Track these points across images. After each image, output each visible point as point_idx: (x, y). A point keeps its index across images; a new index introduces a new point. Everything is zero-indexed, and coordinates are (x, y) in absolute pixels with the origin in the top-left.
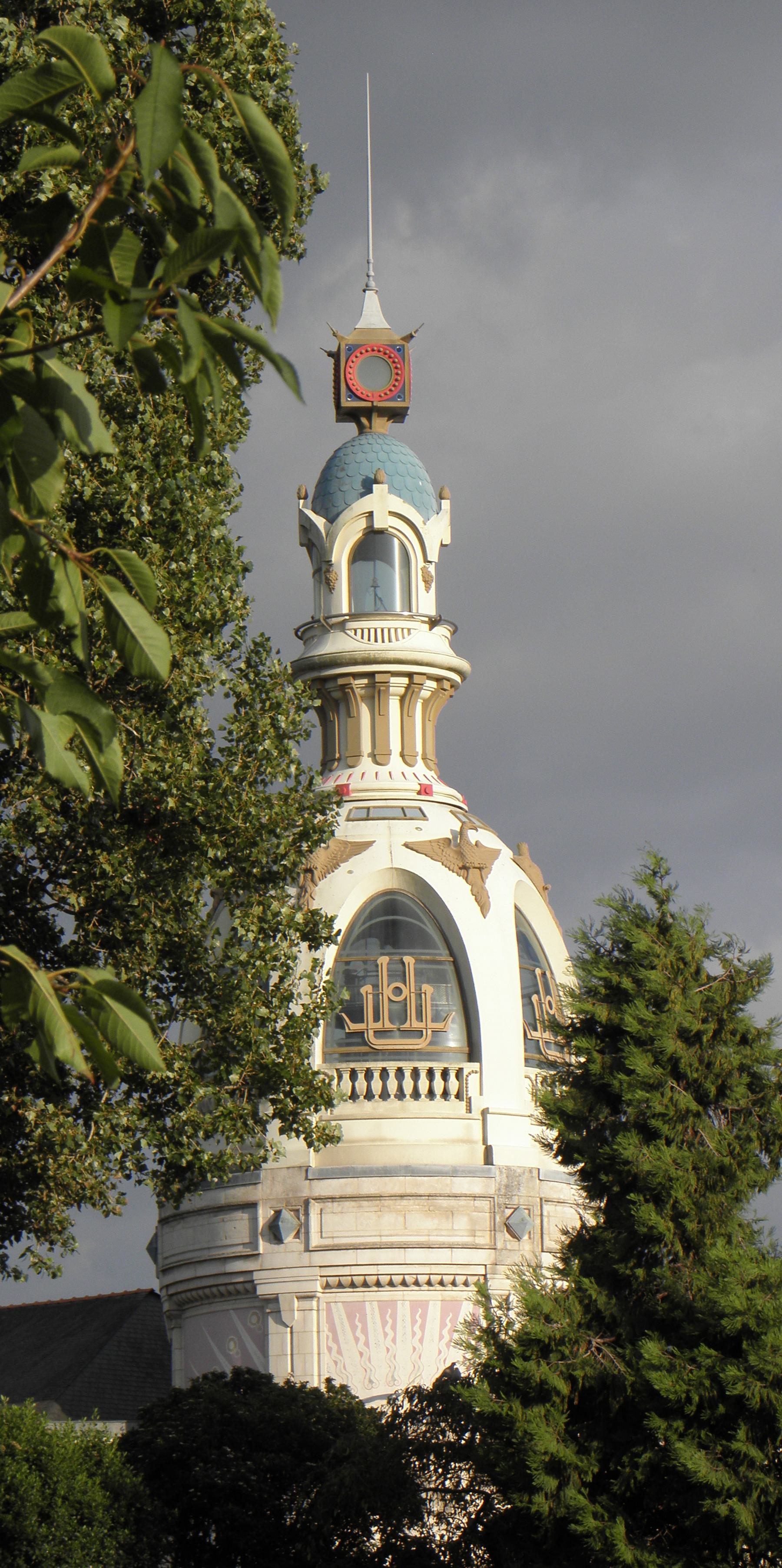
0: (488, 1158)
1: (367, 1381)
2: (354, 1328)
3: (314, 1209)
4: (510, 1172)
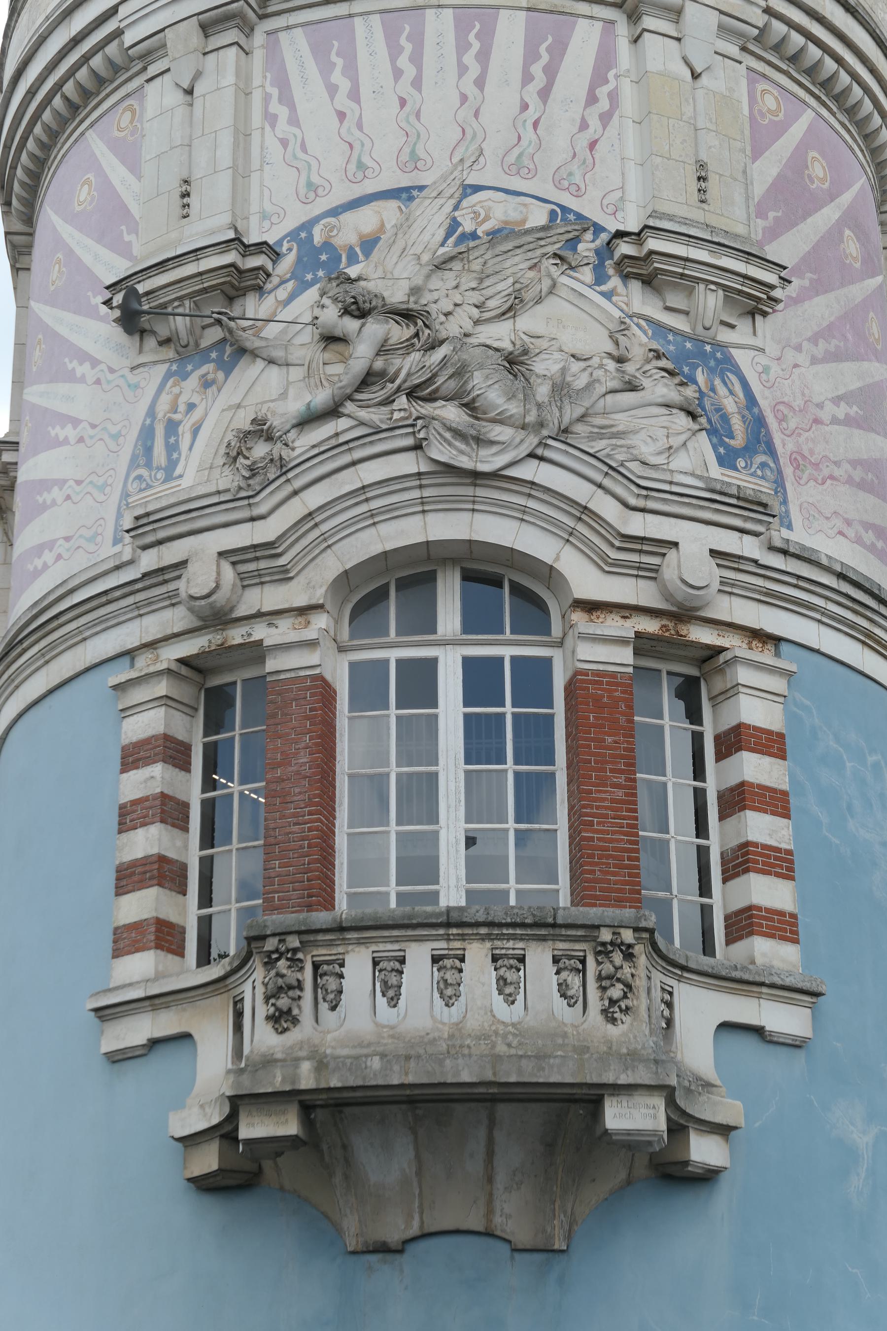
1: (352, 167)
2: (326, 68)
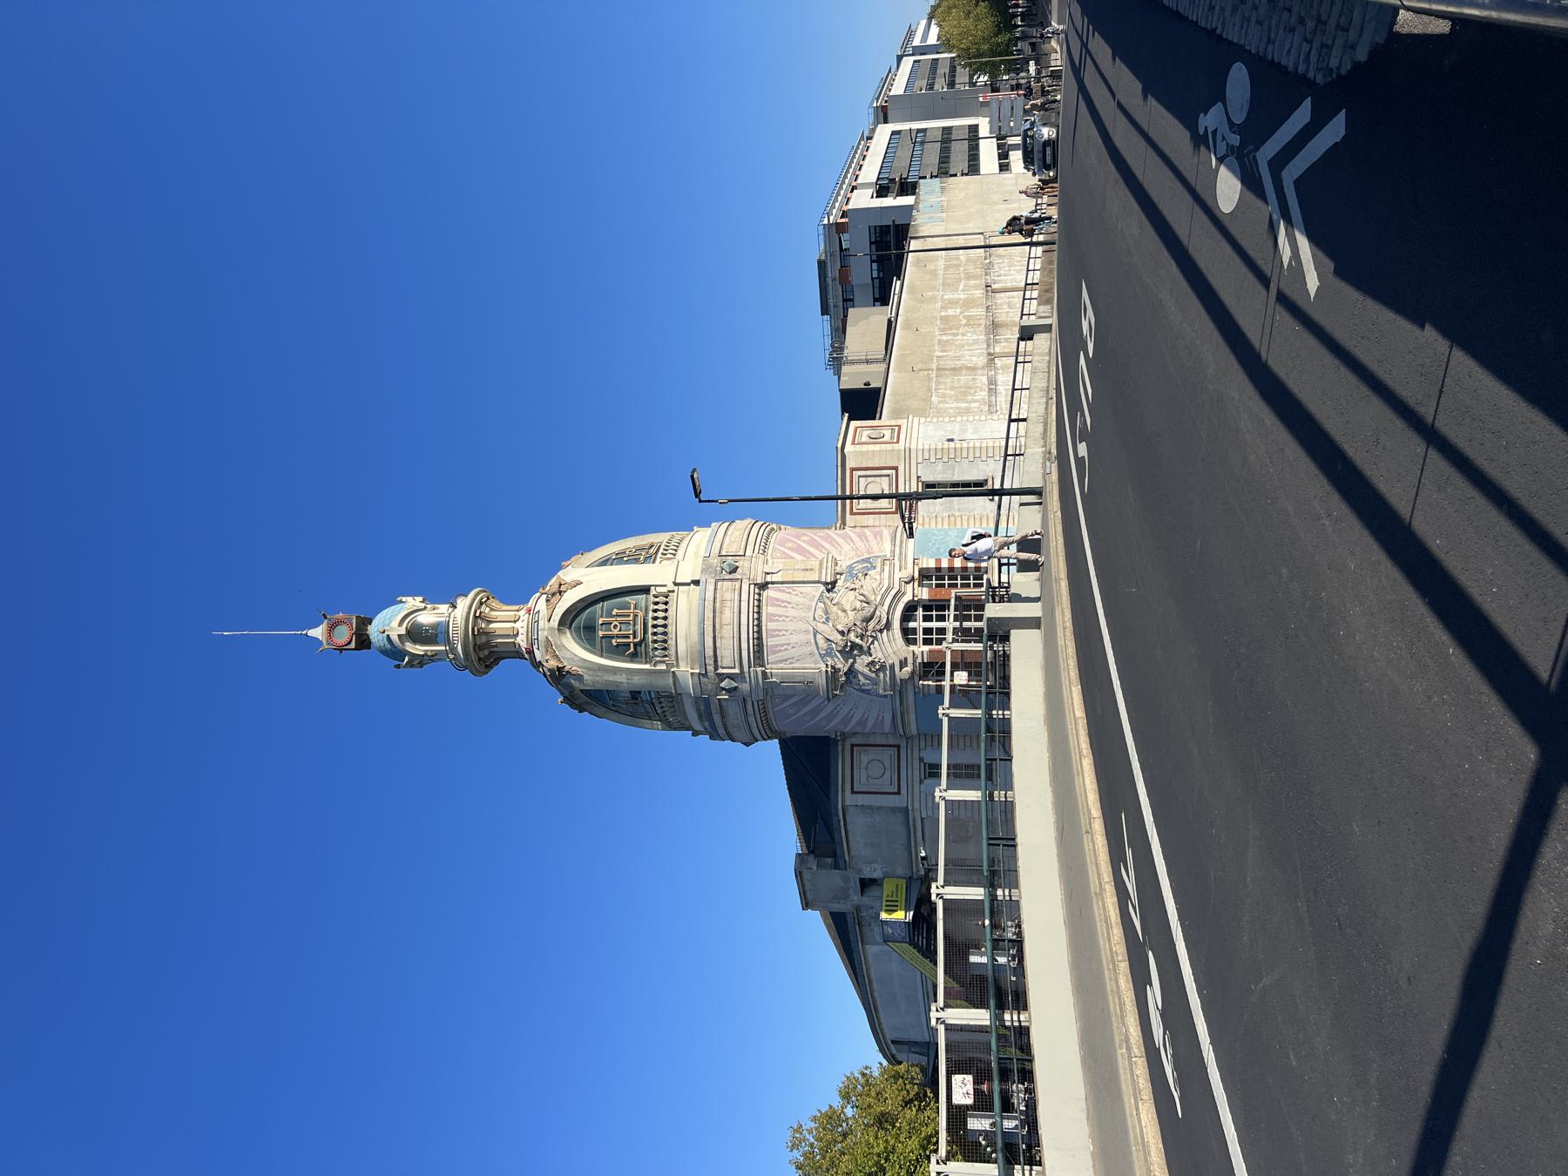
0: (696, 583)
3: (720, 671)
4: (704, 571)
